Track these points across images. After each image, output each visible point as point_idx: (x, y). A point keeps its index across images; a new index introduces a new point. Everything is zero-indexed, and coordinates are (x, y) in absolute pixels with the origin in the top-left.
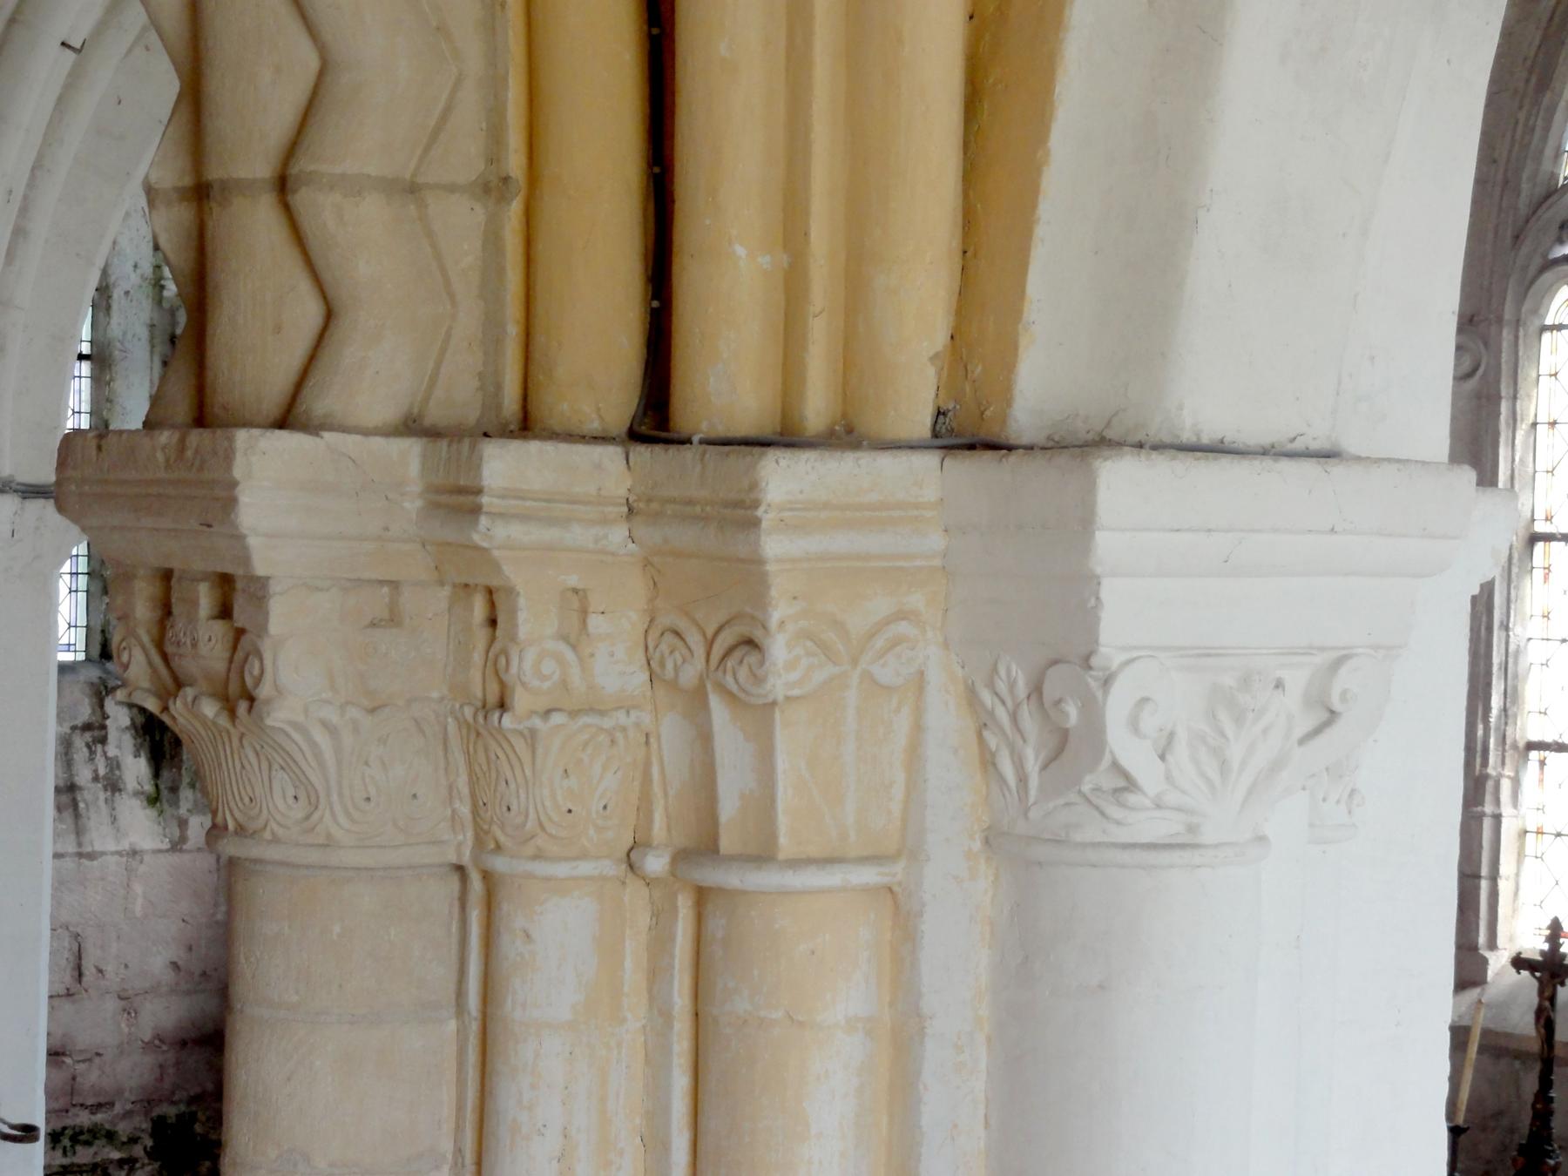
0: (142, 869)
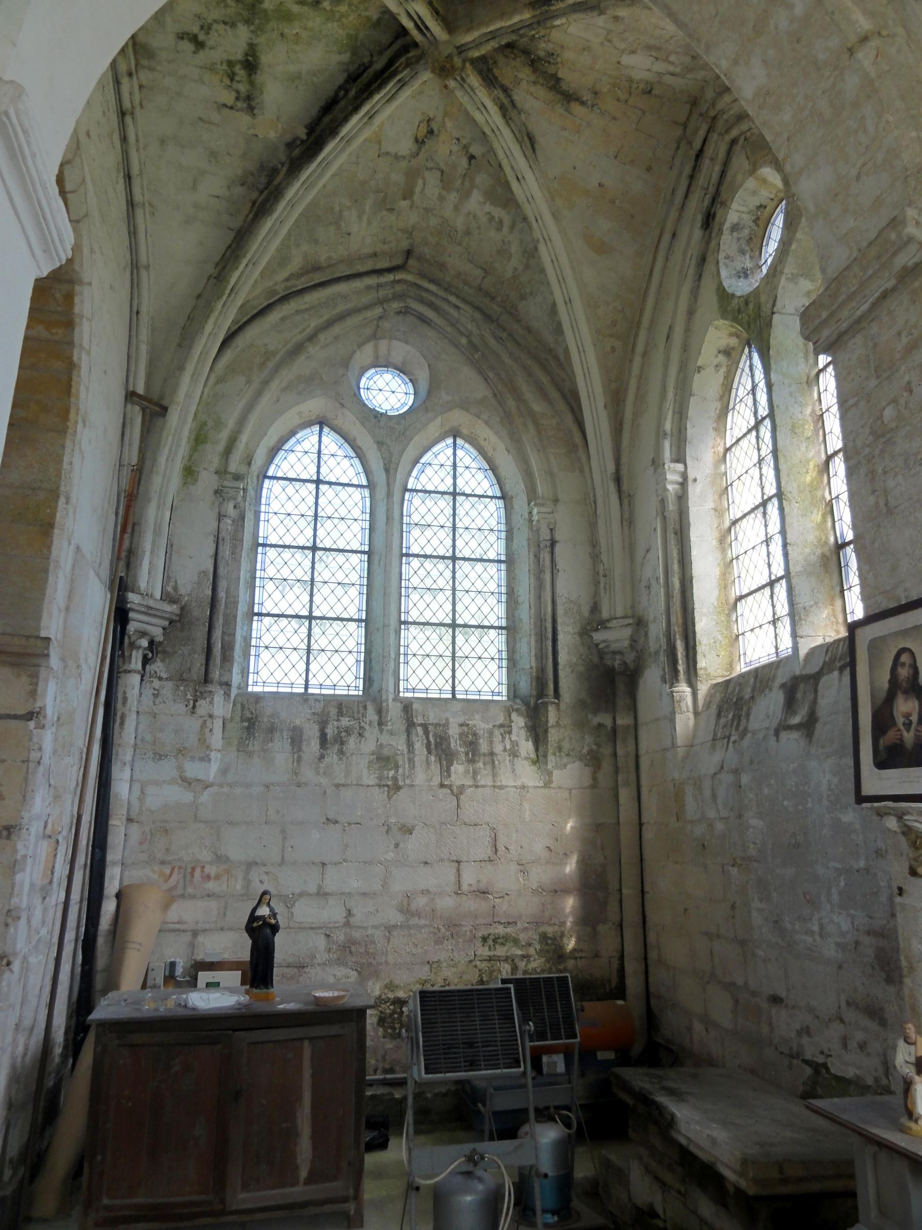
0: (528, 795)
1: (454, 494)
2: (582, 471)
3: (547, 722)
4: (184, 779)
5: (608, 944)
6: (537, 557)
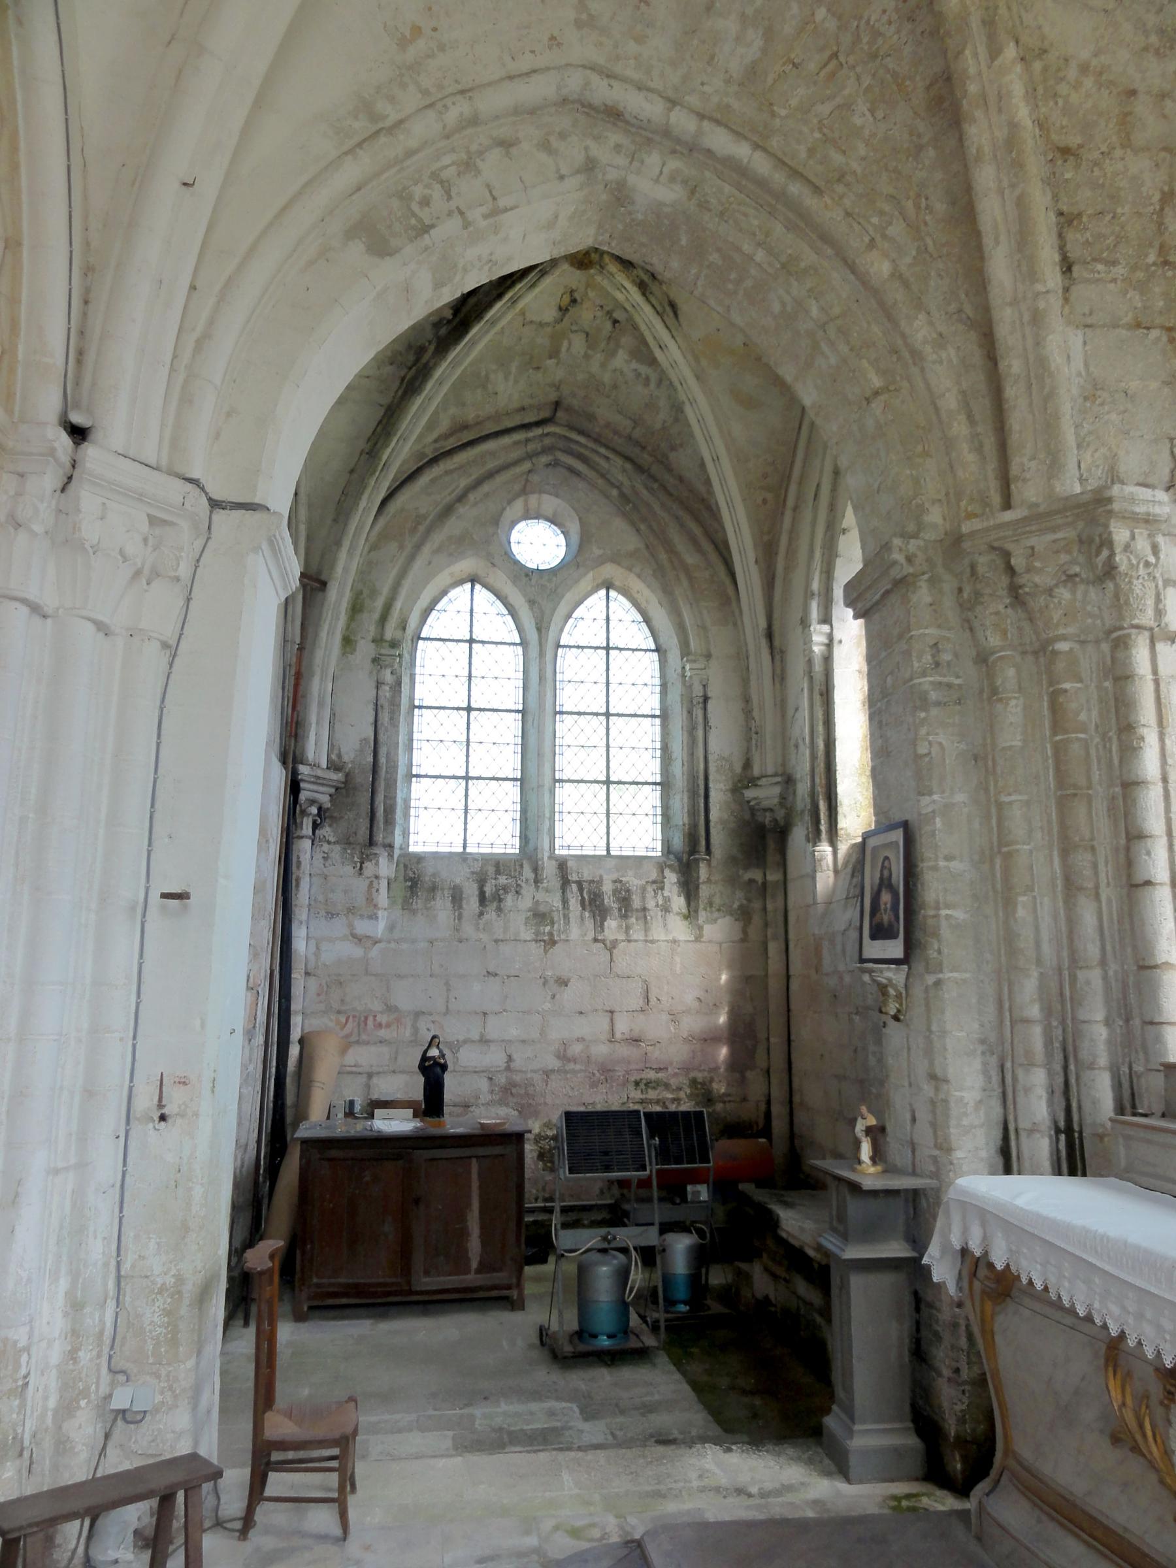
1: (608, 648)
2: (735, 624)
3: (698, 877)
4: (354, 936)
5: (756, 1088)
6: (690, 712)
